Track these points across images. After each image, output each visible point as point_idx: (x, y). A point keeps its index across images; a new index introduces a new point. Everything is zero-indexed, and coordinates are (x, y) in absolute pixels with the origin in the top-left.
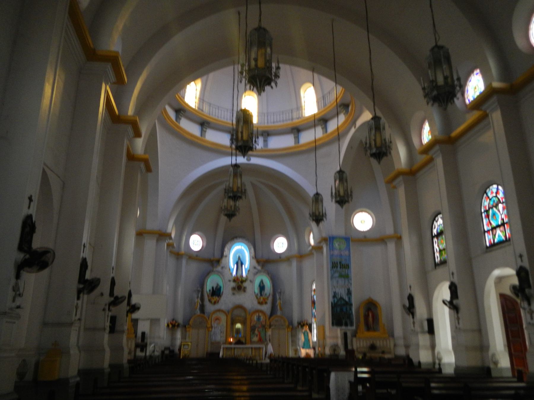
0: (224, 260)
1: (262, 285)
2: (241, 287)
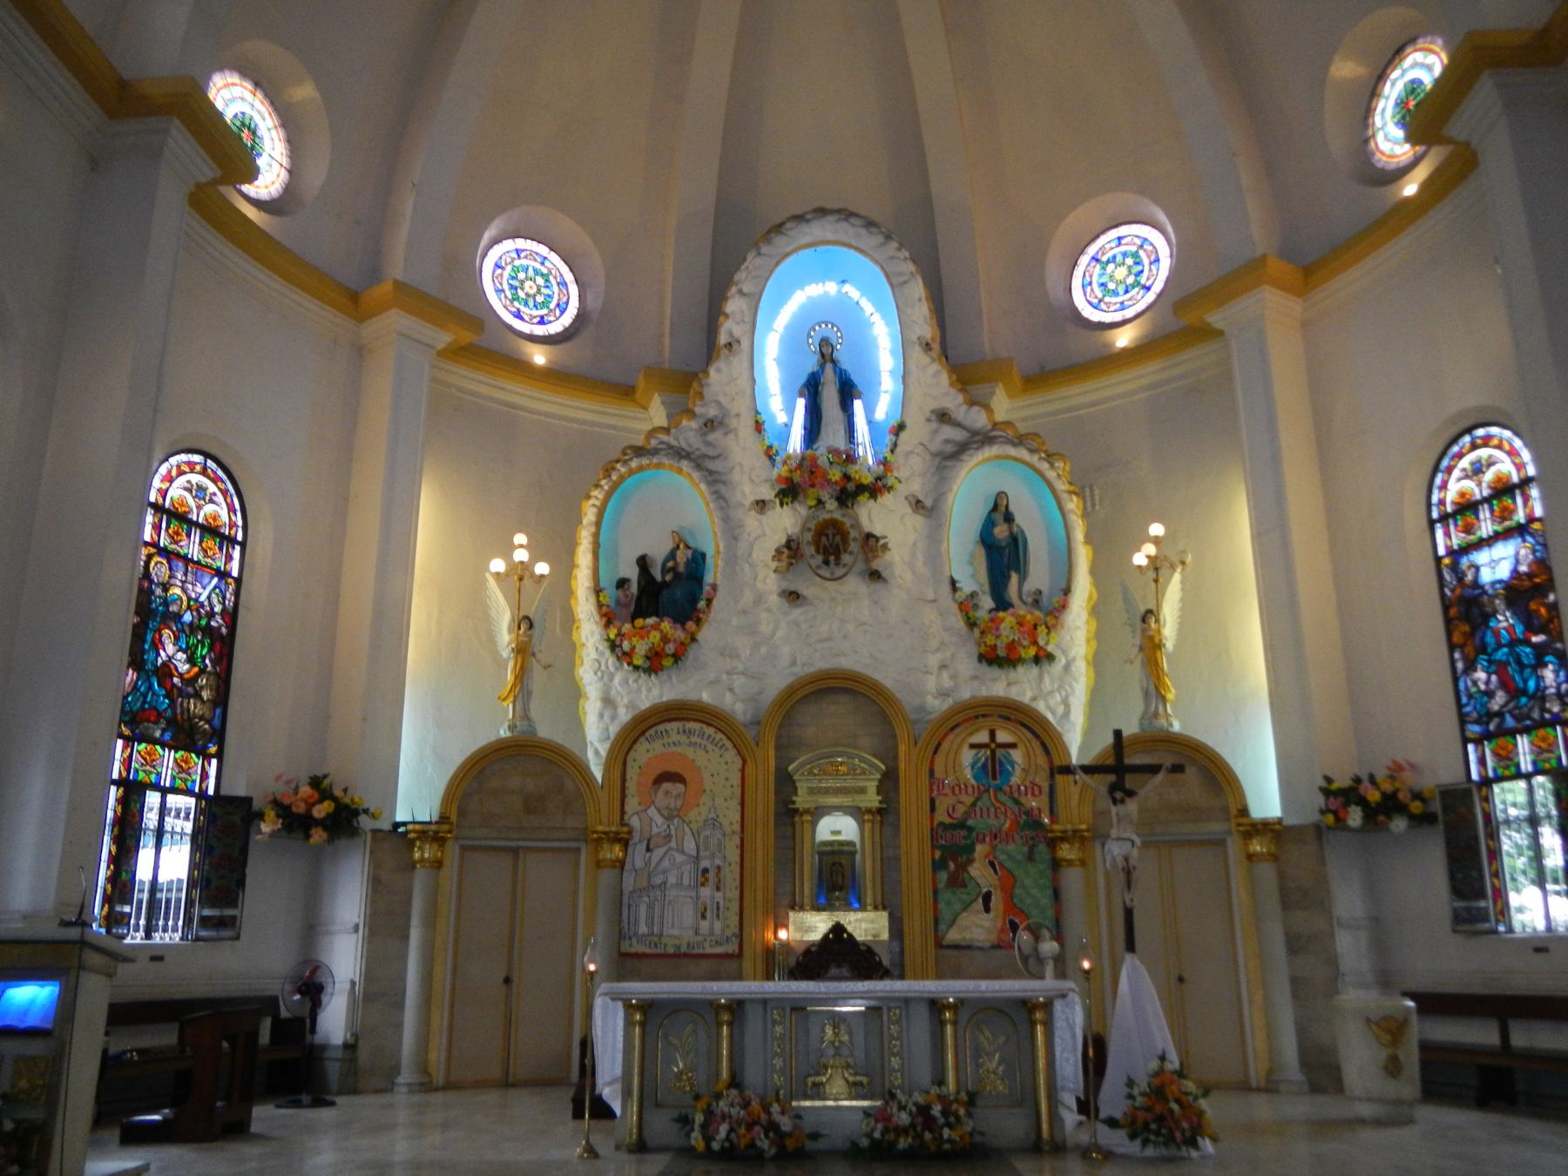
0: (718, 377)
1: (1001, 531)
2: (845, 537)
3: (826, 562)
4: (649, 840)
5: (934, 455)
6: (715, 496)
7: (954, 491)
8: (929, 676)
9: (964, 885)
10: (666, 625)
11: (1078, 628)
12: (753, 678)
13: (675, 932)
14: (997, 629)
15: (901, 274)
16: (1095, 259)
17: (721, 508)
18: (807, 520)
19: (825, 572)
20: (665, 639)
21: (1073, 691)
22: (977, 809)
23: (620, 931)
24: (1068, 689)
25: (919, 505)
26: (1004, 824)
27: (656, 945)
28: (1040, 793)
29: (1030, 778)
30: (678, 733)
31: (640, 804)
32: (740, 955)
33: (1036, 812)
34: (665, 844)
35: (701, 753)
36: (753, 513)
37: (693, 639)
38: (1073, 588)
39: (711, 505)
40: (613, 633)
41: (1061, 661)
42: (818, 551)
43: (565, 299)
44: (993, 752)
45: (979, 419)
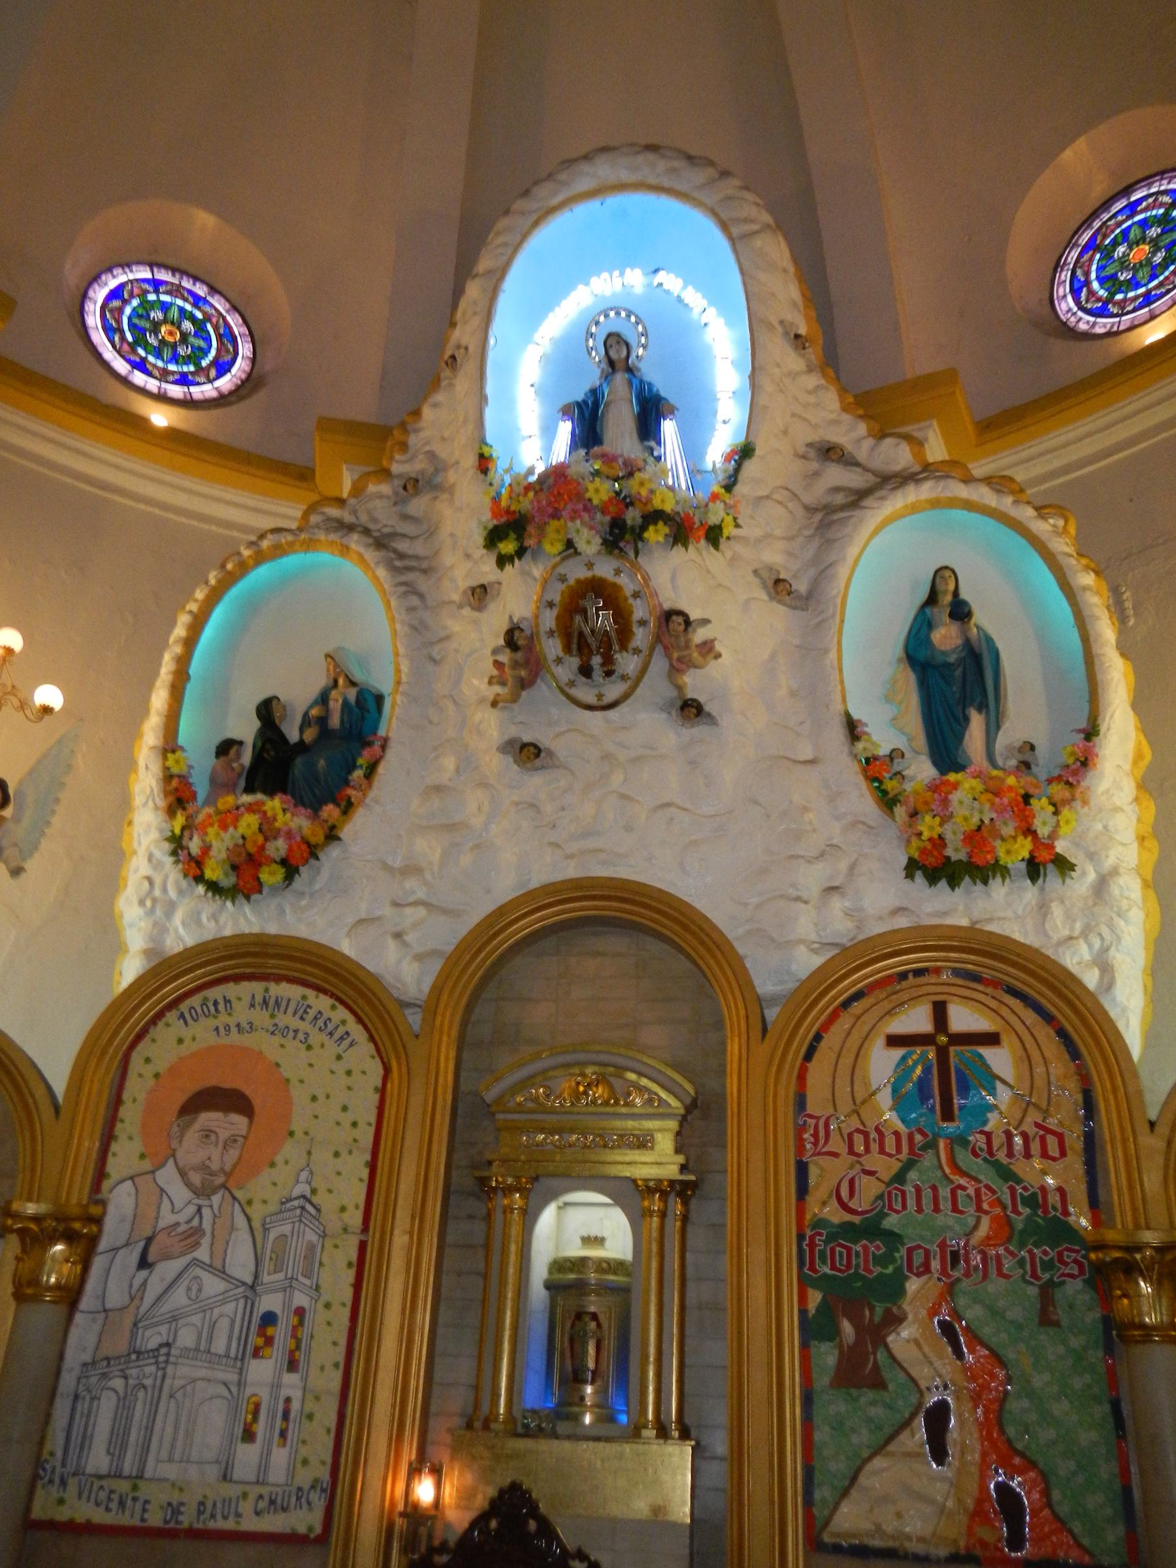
1: (945, 637)
3: (586, 671)
4: (149, 1241)
5: (810, 510)
6: (404, 589)
7: (850, 561)
8: (803, 906)
9: (878, 1383)
10: (274, 804)
11: (1117, 809)
12: (445, 911)
13: (170, 1471)
14: (945, 802)
15: (746, 220)
16: (1091, 246)
17: (411, 609)
18: (545, 583)
19: (586, 694)
20: (267, 830)
21: (1119, 939)
22: (909, 1189)
23: (39, 1462)
24: (1105, 931)
25: (781, 586)
26: (976, 1227)
27: (122, 1504)
28: (1063, 1153)
29: (1033, 1116)
30: (252, 1006)
31: (142, 1156)
32: (323, 1539)
33: (1054, 1199)
34: (182, 1254)
35: (292, 1045)
36: (467, 611)
37: (332, 836)
38: (1103, 729)
39: (393, 603)
40: (180, 821)
41: (1086, 877)
42: (567, 649)
43: (228, 358)
44: (942, 1053)
45: (898, 456)
